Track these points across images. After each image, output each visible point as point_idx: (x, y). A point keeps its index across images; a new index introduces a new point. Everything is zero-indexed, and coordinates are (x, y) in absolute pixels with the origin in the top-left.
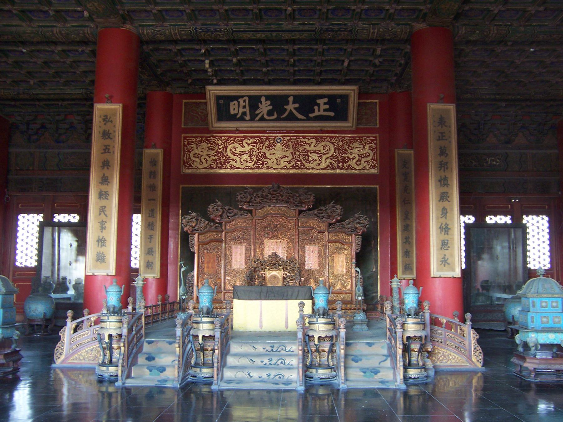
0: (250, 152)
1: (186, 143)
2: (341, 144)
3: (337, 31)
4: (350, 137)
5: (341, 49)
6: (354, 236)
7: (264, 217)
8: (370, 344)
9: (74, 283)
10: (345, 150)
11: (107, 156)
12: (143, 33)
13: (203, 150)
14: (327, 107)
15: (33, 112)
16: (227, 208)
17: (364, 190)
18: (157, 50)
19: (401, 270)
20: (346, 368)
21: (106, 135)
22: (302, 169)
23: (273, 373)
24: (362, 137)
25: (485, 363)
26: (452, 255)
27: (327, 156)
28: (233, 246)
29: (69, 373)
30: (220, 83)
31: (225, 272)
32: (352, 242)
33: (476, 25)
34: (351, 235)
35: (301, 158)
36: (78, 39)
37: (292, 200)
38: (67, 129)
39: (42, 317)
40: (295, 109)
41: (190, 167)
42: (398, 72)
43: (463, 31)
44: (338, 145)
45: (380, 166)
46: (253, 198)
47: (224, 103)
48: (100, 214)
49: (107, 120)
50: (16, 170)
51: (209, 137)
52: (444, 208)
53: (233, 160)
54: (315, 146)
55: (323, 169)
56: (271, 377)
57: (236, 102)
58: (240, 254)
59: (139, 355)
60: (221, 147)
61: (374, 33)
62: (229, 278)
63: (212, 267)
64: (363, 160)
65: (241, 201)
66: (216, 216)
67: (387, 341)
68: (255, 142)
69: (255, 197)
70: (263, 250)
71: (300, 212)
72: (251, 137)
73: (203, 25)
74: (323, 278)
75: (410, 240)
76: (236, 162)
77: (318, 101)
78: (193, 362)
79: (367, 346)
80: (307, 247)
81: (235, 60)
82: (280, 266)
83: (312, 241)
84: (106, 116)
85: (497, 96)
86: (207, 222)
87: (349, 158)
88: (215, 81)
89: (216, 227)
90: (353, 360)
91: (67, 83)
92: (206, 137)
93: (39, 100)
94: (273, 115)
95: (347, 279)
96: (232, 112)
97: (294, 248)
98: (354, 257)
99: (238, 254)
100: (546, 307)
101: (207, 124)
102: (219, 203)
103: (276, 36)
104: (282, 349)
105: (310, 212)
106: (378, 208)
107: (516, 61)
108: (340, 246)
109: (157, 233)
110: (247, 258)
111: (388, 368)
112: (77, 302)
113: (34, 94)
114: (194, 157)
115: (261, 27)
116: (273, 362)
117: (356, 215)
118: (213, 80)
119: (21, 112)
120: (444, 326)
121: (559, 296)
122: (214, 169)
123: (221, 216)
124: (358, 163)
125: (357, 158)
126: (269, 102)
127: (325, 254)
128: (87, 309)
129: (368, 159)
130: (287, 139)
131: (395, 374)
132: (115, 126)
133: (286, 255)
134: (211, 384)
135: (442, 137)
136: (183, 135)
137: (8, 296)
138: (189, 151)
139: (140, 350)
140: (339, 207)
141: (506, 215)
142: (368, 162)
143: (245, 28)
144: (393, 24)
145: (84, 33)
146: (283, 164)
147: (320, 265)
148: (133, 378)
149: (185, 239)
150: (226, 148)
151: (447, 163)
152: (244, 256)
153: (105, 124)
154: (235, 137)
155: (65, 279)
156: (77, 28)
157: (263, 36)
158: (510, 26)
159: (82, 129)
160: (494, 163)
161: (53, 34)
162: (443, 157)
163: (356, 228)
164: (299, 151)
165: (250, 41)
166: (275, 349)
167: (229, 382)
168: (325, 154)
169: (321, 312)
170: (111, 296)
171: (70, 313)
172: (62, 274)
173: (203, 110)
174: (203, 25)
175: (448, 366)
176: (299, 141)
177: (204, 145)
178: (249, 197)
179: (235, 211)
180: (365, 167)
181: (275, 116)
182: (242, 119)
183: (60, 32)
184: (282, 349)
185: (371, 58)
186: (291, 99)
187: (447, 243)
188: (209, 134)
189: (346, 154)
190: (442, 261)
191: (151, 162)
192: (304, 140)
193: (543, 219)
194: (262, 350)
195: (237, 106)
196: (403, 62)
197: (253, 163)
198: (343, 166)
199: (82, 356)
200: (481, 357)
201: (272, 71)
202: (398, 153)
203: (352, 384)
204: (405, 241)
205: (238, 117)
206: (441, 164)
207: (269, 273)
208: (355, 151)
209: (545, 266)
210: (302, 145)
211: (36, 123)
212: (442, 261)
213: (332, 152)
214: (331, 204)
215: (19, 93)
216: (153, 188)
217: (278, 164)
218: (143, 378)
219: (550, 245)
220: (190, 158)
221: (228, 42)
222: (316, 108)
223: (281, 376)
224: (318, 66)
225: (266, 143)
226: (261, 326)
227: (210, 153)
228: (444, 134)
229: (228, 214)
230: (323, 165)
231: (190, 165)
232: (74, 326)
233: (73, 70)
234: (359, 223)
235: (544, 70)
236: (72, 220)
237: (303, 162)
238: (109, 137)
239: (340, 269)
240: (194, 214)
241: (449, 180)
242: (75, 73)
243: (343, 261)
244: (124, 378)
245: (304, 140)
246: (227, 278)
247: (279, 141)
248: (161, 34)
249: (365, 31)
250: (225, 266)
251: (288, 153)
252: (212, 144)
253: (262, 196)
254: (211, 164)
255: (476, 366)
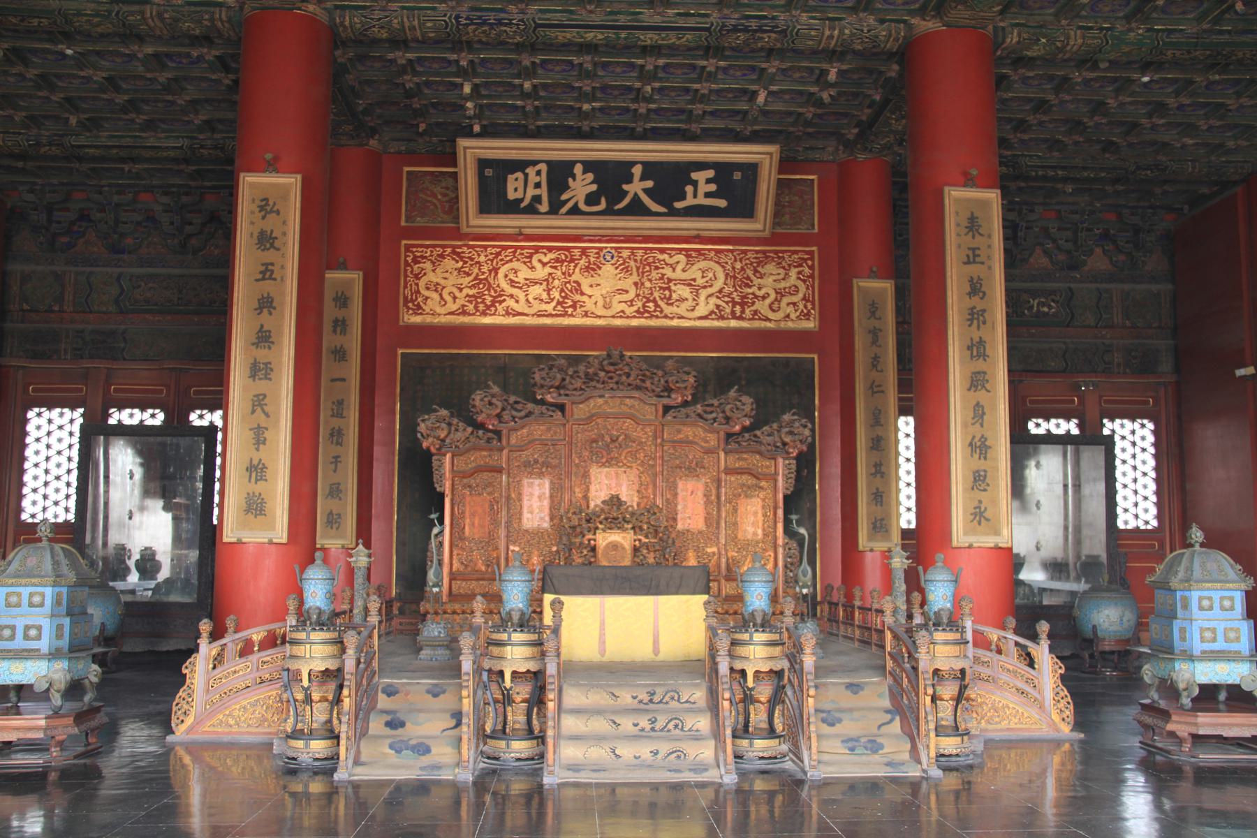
0: (548, 280)
1: (409, 259)
2: (738, 265)
3: (756, 31)
4: (757, 252)
5: (753, 69)
6: (780, 461)
7: (590, 418)
8: (854, 688)
9: (138, 557)
10: (748, 278)
11: (268, 286)
12: (342, 24)
13: (447, 275)
14: (713, 187)
15: (63, 184)
16: (512, 399)
17: (787, 362)
18: (362, 58)
19: (865, 531)
20: (819, 737)
21: (266, 240)
22: (657, 317)
23: (664, 748)
24: (783, 252)
25: (1079, 725)
26: (995, 502)
27: (710, 291)
28: (525, 481)
29: (207, 756)
30: (485, 133)
31: (507, 536)
32: (776, 473)
33: (1041, 27)
34: (775, 459)
35: (656, 295)
36: (197, 32)
37: (648, 384)
38: (139, 223)
39: (97, 633)
40: (646, 191)
41: (418, 309)
42: (864, 118)
43: (1013, 38)
44: (734, 268)
45: (821, 314)
46: (568, 379)
47: (494, 176)
48: (253, 412)
49: (269, 208)
50: (23, 311)
51: (460, 247)
52: (978, 404)
53: (512, 296)
54: (684, 271)
55: (701, 318)
56: (659, 756)
57: (519, 175)
58: (540, 497)
59: (372, 716)
60: (485, 269)
61: (831, 37)
62: (517, 549)
63: (482, 526)
64: (785, 300)
65: (542, 386)
66: (489, 416)
67: (889, 680)
68: (557, 260)
69: (571, 377)
70: (588, 489)
71: (667, 409)
72: (550, 249)
73: (473, 9)
74: (715, 549)
75: (883, 469)
76: (517, 302)
77: (694, 176)
78: (488, 729)
79: (849, 693)
80: (680, 484)
81: (527, 85)
82: (628, 522)
83: (692, 470)
84: (266, 200)
85: (1060, 173)
86: (470, 429)
87: (756, 297)
88: (477, 128)
89: (488, 441)
90: (824, 721)
91: (150, 125)
92: (454, 247)
93: (80, 159)
94: (598, 203)
95: (765, 550)
96: (511, 195)
97: (655, 485)
98: (781, 504)
99: (535, 499)
100: (1211, 608)
101: (457, 219)
102: (496, 389)
103: (625, 39)
104: (673, 698)
105: (689, 410)
106: (817, 402)
107: (1109, 101)
108: (751, 481)
109: (351, 451)
110: (554, 507)
111: (896, 736)
112: (165, 599)
113: (73, 146)
114: (428, 289)
115: (597, 19)
116: (658, 726)
117: (786, 417)
118: (471, 126)
119: (35, 184)
120: (993, 647)
121: (1237, 585)
122: (470, 314)
123: (499, 416)
124: (775, 306)
125: (773, 296)
126: (590, 177)
127: (718, 497)
128: (232, 617)
129: (794, 299)
130: (626, 253)
131: (914, 750)
132: (284, 223)
133: (636, 499)
134: (537, 773)
135: (972, 257)
136: (404, 242)
137: (78, 589)
138: (417, 277)
139: (372, 707)
140: (747, 400)
141: (1068, 419)
142: (794, 304)
143: (563, 18)
144: (871, 20)
145: (212, 20)
146: (617, 307)
147: (707, 520)
148: (363, 764)
149: (417, 465)
150: (496, 270)
151: (984, 311)
152: (546, 503)
153: (264, 218)
154: (516, 248)
155: (122, 551)
156: (198, 9)
157: (600, 37)
158: (1107, 29)
159: (172, 223)
160: (1046, 309)
161: (144, 18)
162: (975, 301)
163: (785, 444)
164: (650, 280)
165: (567, 46)
166: (656, 698)
167: (574, 768)
168: (705, 287)
169: (759, 621)
170: (312, 588)
171: (205, 626)
172: (115, 538)
173: (447, 188)
174: (473, 9)
175: (1001, 730)
176: (651, 260)
177: (449, 263)
178: (559, 376)
179: (530, 406)
180: (788, 316)
181: (603, 205)
182: (531, 210)
183: (160, 15)
184: (673, 698)
185: (813, 89)
186: (637, 171)
187: (985, 477)
188: (460, 240)
189: (750, 287)
190: (975, 514)
191: (336, 299)
192: (661, 257)
193: (1143, 426)
194: (629, 700)
195: (522, 184)
196: (877, 98)
197: (554, 304)
198: (743, 312)
199: (233, 717)
200: (1069, 713)
201: (601, 109)
202: (858, 287)
203: (830, 769)
204: (873, 470)
205: (523, 205)
206: (972, 314)
207: (604, 539)
208: (769, 281)
209: (1147, 523)
210: (657, 268)
211: (67, 210)
212: (975, 514)
213: (719, 284)
214: (732, 393)
215: (38, 144)
216: (340, 354)
217: (607, 306)
218: (376, 763)
219: (1158, 480)
220: (418, 292)
221: (519, 48)
222: (689, 189)
223: (680, 754)
224: (701, 102)
225: (582, 262)
226: (603, 651)
227: (461, 281)
228: (977, 252)
229: (515, 413)
230: (702, 310)
231: (419, 307)
232: (214, 652)
233: (170, 98)
234: (791, 433)
235: (1162, 121)
236: (150, 422)
237: (660, 302)
238: (272, 246)
239: (750, 529)
240: (444, 412)
241: (987, 346)
242: (173, 103)
243: (755, 513)
244: (350, 762)
245: (661, 257)
246: (512, 548)
247: (608, 258)
248: (382, 27)
249: (813, 33)
250: (508, 524)
251: (628, 283)
252: (465, 263)
253: (587, 374)
254: (463, 306)
255: (1058, 730)
